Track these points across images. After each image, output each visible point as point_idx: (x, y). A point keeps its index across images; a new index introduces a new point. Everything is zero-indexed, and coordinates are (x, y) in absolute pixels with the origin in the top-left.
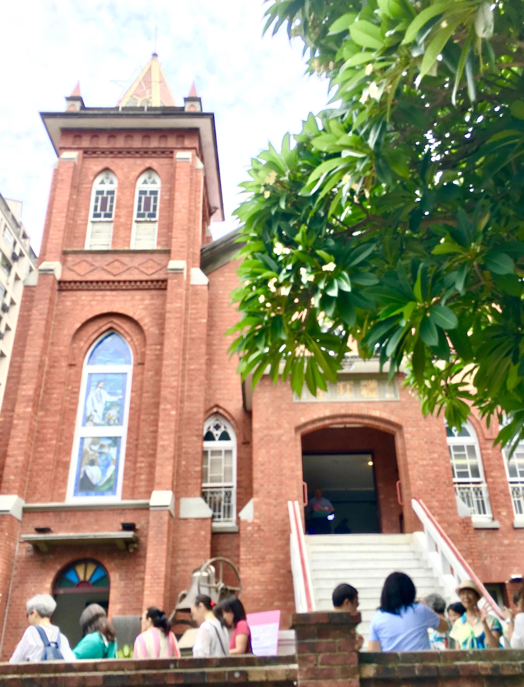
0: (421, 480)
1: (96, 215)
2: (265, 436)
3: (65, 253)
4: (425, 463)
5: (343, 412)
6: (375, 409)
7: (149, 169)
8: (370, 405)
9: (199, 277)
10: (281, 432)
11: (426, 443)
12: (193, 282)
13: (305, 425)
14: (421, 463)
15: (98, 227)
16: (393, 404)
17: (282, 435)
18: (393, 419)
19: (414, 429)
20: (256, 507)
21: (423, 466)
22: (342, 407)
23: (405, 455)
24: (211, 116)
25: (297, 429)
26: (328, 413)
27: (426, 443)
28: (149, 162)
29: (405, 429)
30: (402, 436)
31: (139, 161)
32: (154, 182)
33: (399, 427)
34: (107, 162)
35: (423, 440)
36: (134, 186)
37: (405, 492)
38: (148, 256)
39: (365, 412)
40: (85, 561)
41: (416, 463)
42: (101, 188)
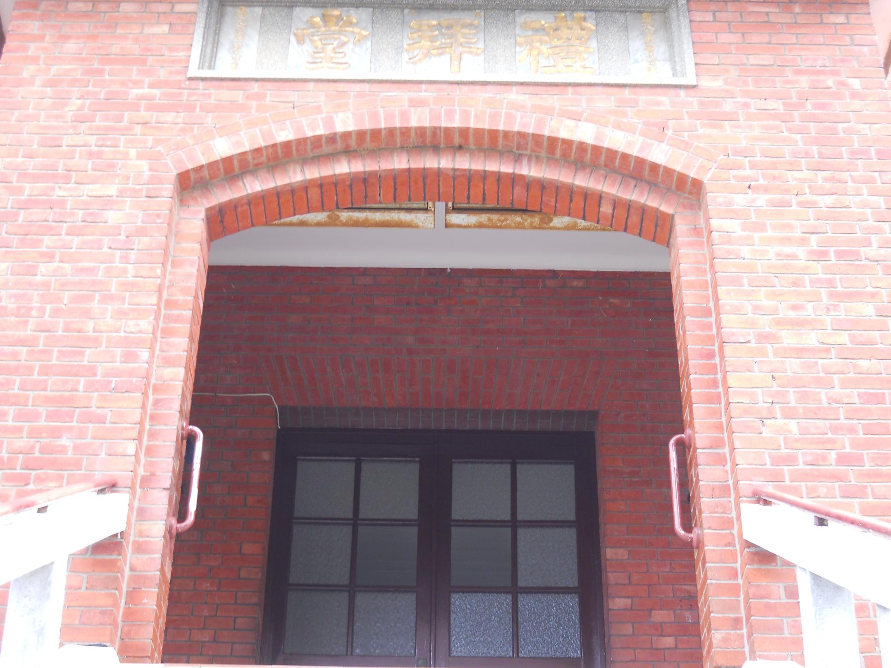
0: (789, 414)
2: (25, 205)
4: (811, 339)
5: (418, 119)
6: (576, 117)
8: (553, 100)
10: (112, 190)
11: (820, 255)
13: (231, 169)
14: (788, 338)
16: (665, 100)
17: (107, 202)
18: (659, 154)
19: (762, 200)
21: (800, 352)
22: (414, 103)
23: (712, 310)
25: (189, 183)
26: (345, 122)
27: (820, 255)
29: (714, 198)
30: (702, 233)
33: (689, 189)
35: (803, 242)
37: (706, 475)
39: (524, 122)
41: (764, 338)
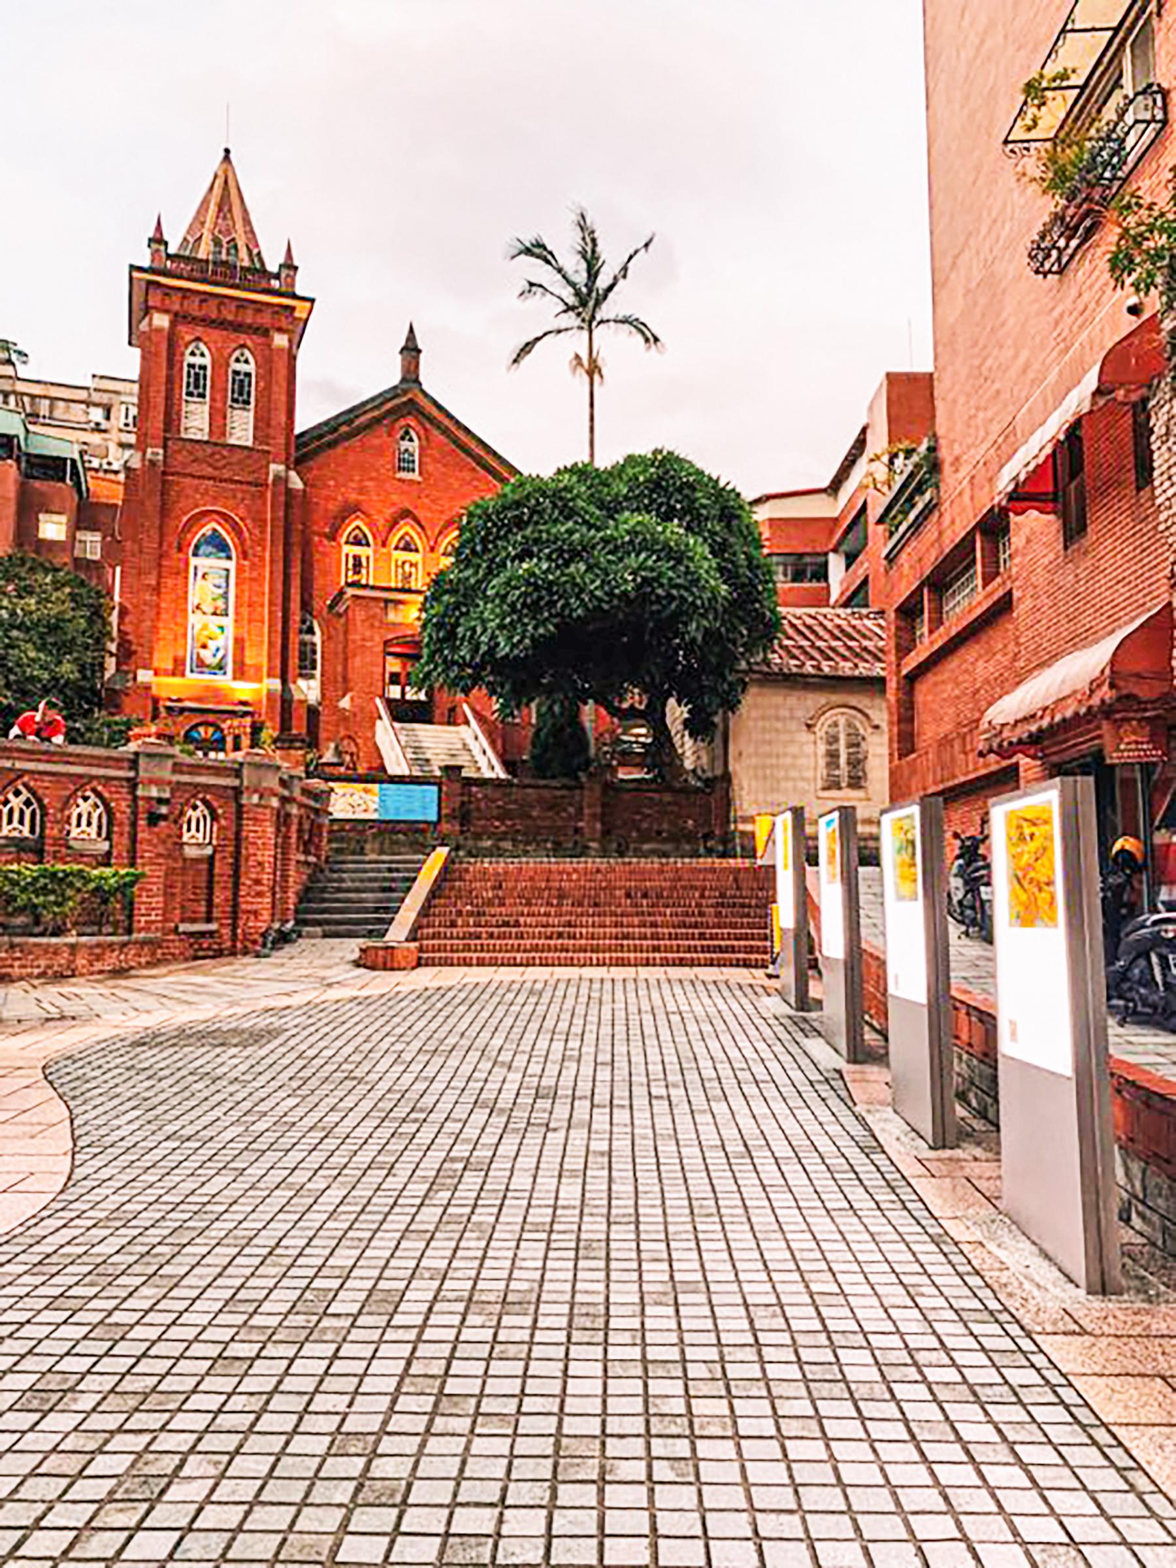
1: (190, 394)
3: (166, 439)
7: (243, 346)
9: (296, 483)
12: (291, 486)
15: (192, 407)
20: (352, 699)
24: (312, 301)
28: (243, 338)
31: (233, 336)
32: (246, 362)
34: (199, 331)
36: (228, 365)
38: (246, 452)
40: (207, 724)
42: (192, 360)
